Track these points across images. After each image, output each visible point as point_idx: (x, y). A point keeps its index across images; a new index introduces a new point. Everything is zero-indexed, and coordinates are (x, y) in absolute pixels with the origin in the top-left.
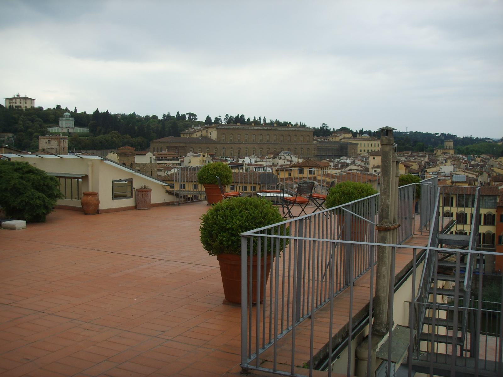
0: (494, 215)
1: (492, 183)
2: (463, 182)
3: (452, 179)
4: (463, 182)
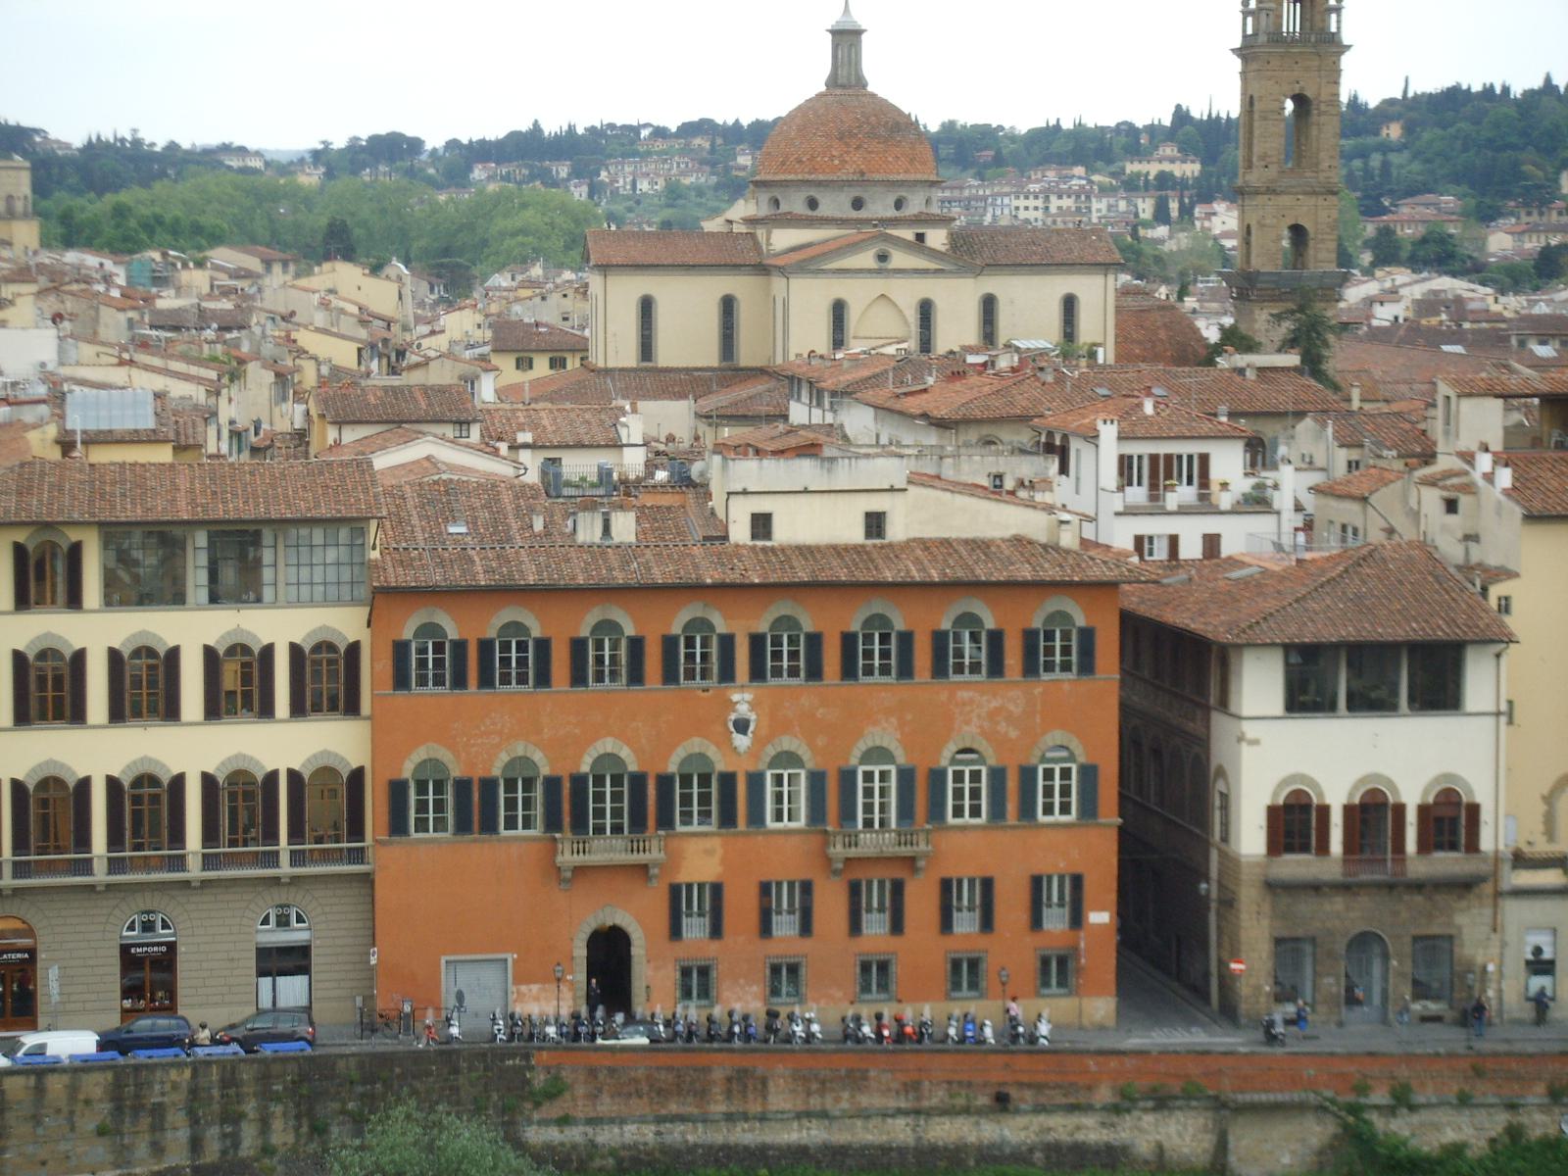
0: (354, 649)
1: (324, 437)
2: (135, 438)
3: (62, 417)
4: (135, 438)
